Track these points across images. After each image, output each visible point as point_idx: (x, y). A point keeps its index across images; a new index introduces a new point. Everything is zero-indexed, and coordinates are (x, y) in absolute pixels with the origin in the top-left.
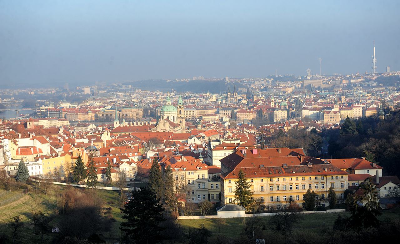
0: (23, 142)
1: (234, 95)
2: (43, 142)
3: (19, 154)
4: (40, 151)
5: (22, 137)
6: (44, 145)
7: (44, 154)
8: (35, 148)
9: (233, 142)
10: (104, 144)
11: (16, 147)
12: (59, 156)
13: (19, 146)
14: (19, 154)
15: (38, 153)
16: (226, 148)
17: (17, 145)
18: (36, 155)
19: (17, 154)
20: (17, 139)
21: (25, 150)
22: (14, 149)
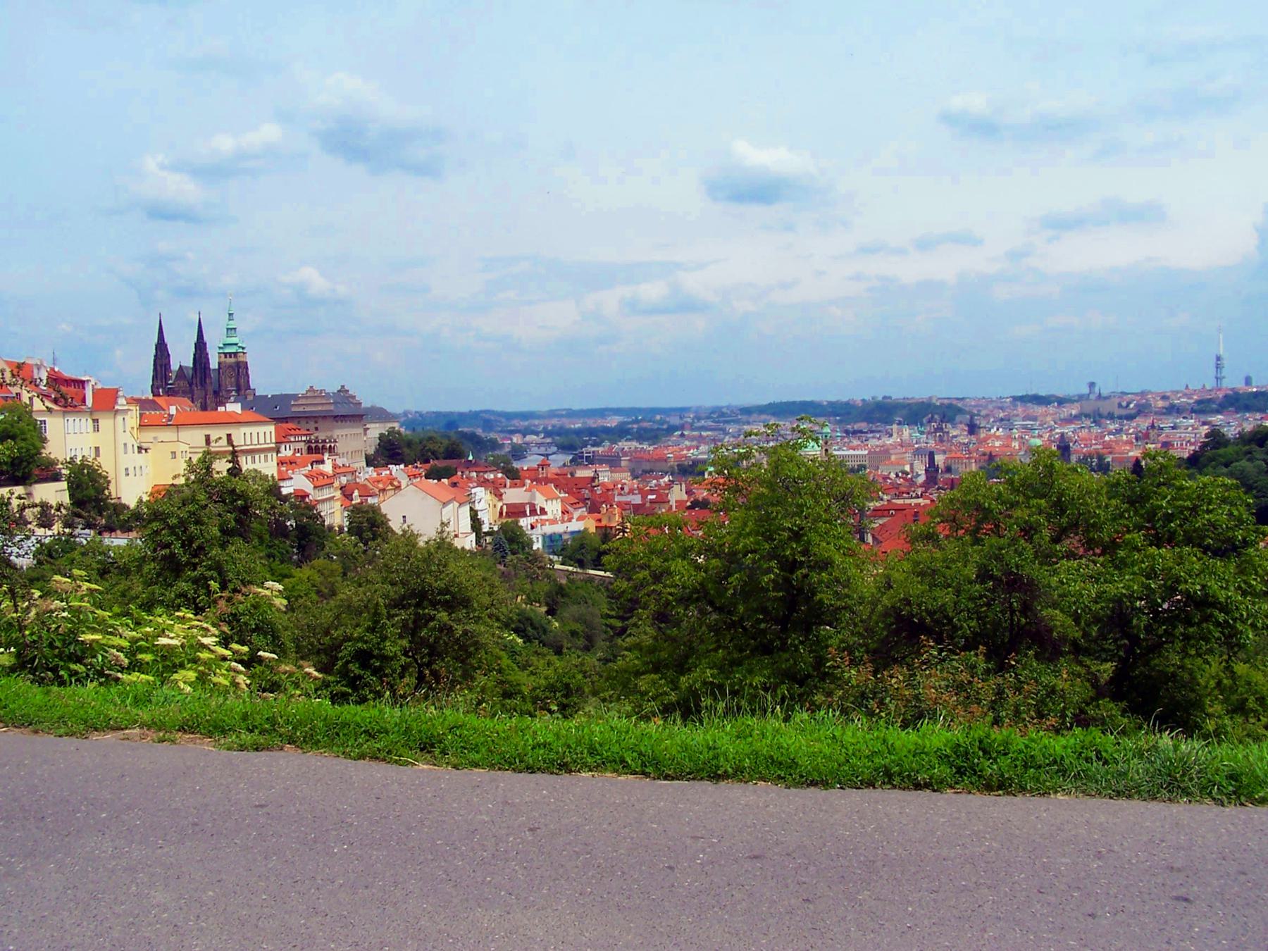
0: (514, 495)
1: (944, 426)
2: (550, 498)
3: (504, 514)
4: (543, 511)
5: (510, 487)
6: (549, 502)
7: (549, 516)
8: (533, 507)
9: (908, 501)
10: (671, 506)
11: (500, 504)
12: (574, 520)
13: (504, 502)
14: (504, 514)
15: (537, 515)
16: (894, 512)
17: (501, 499)
18: (536, 517)
19: (501, 513)
20: (502, 491)
21: (516, 511)
22: (495, 506)
